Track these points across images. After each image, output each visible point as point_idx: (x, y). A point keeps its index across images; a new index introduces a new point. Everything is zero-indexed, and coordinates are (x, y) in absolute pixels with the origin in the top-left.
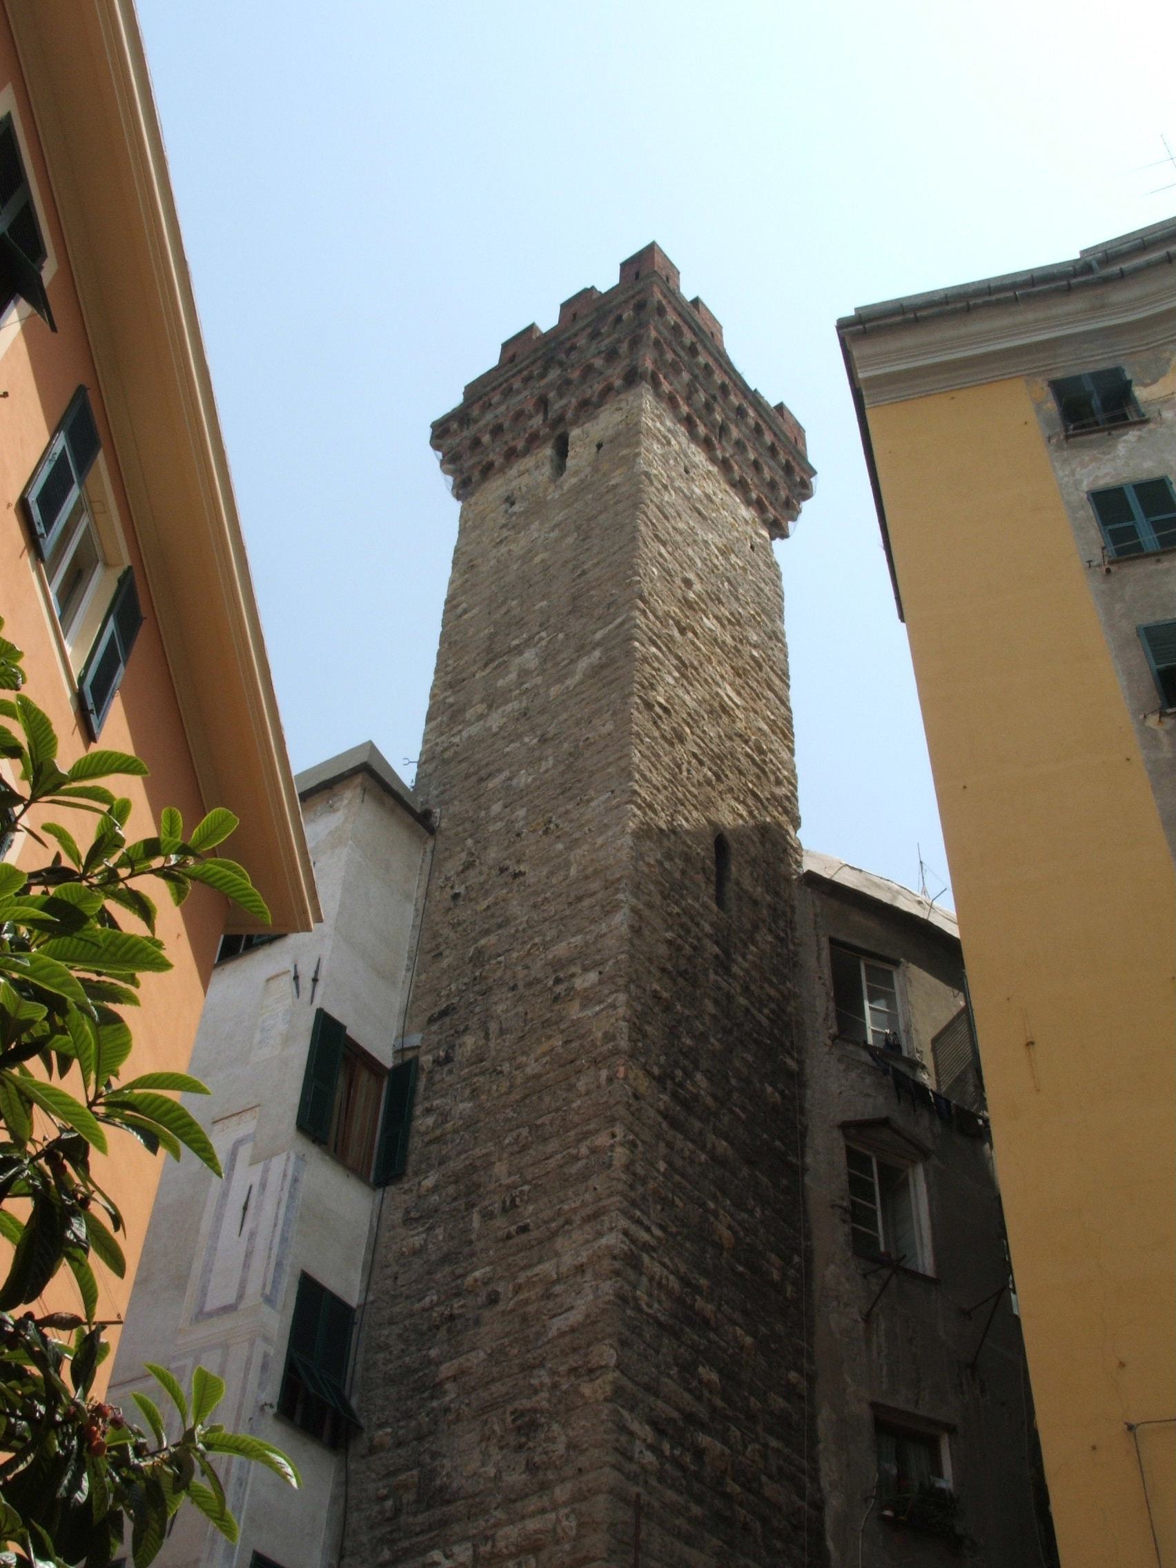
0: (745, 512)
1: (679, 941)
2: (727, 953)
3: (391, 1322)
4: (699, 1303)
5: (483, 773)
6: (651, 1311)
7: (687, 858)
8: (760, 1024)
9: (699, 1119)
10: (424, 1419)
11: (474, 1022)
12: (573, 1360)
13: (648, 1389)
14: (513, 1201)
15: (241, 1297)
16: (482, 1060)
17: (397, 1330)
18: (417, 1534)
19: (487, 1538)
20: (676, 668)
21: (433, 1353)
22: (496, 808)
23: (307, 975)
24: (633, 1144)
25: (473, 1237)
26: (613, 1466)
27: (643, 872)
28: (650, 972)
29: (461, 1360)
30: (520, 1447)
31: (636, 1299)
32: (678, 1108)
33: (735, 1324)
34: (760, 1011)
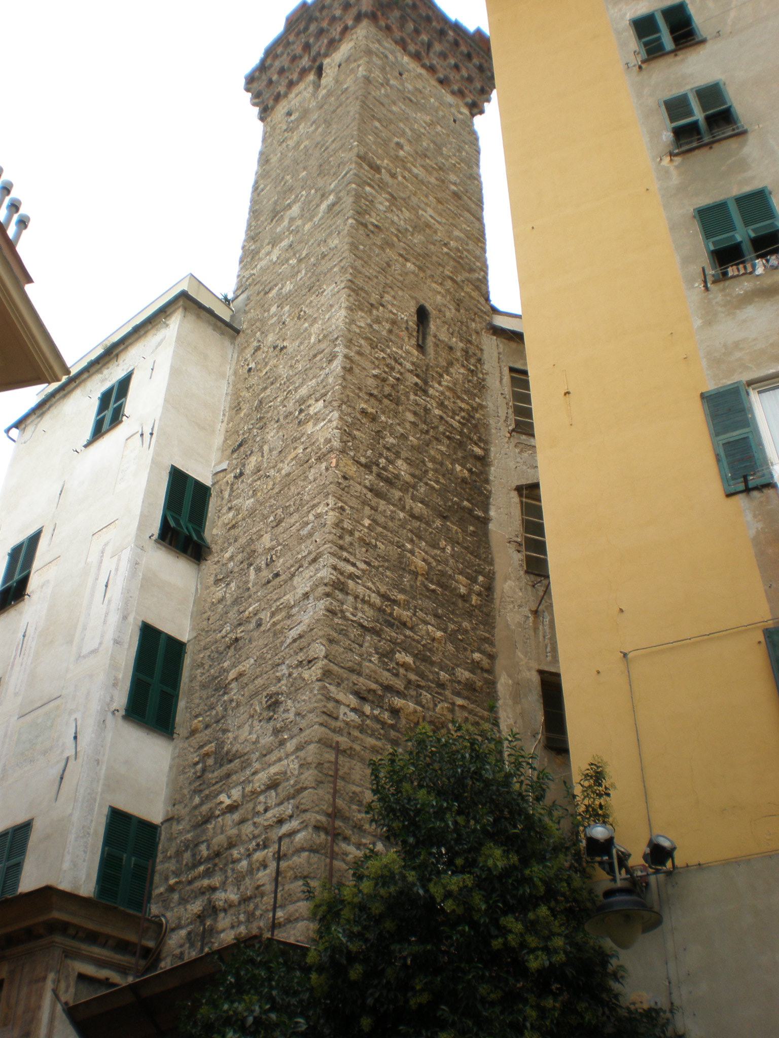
0: (449, 99)
1: (384, 375)
2: (426, 382)
3: (205, 648)
4: (397, 610)
5: (267, 289)
6: (355, 619)
7: (394, 322)
8: (452, 426)
9: (400, 490)
10: (220, 708)
11: (255, 449)
12: (301, 656)
13: (352, 670)
14: (272, 558)
15: (101, 644)
16: (259, 471)
17: (208, 653)
18: (214, 785)
19: (249, 782)
20: (387, 200)
21: (226, 665)
22: (274, 309)
23: (147, 432)
24: (342, 508)
25: (250, 585)
26: (321, 724)
27: (355, 332)
28: (359, 397)
29: (240, 667)
30: (270, 719)
31: (342, 611)
32: (382, 484)
33: (426, 623)
34: (453, 418)
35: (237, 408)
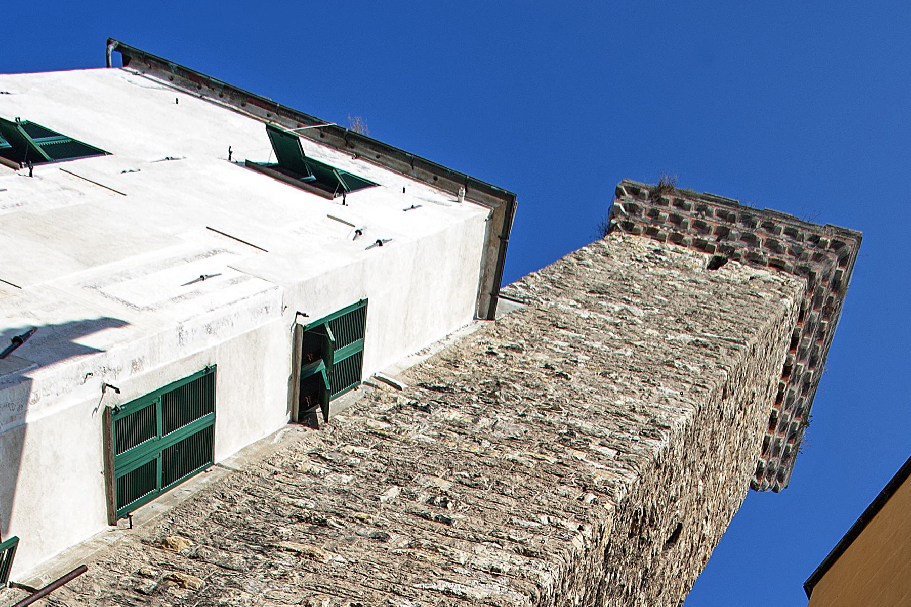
25: (382, 498)
35: (453, 363)
